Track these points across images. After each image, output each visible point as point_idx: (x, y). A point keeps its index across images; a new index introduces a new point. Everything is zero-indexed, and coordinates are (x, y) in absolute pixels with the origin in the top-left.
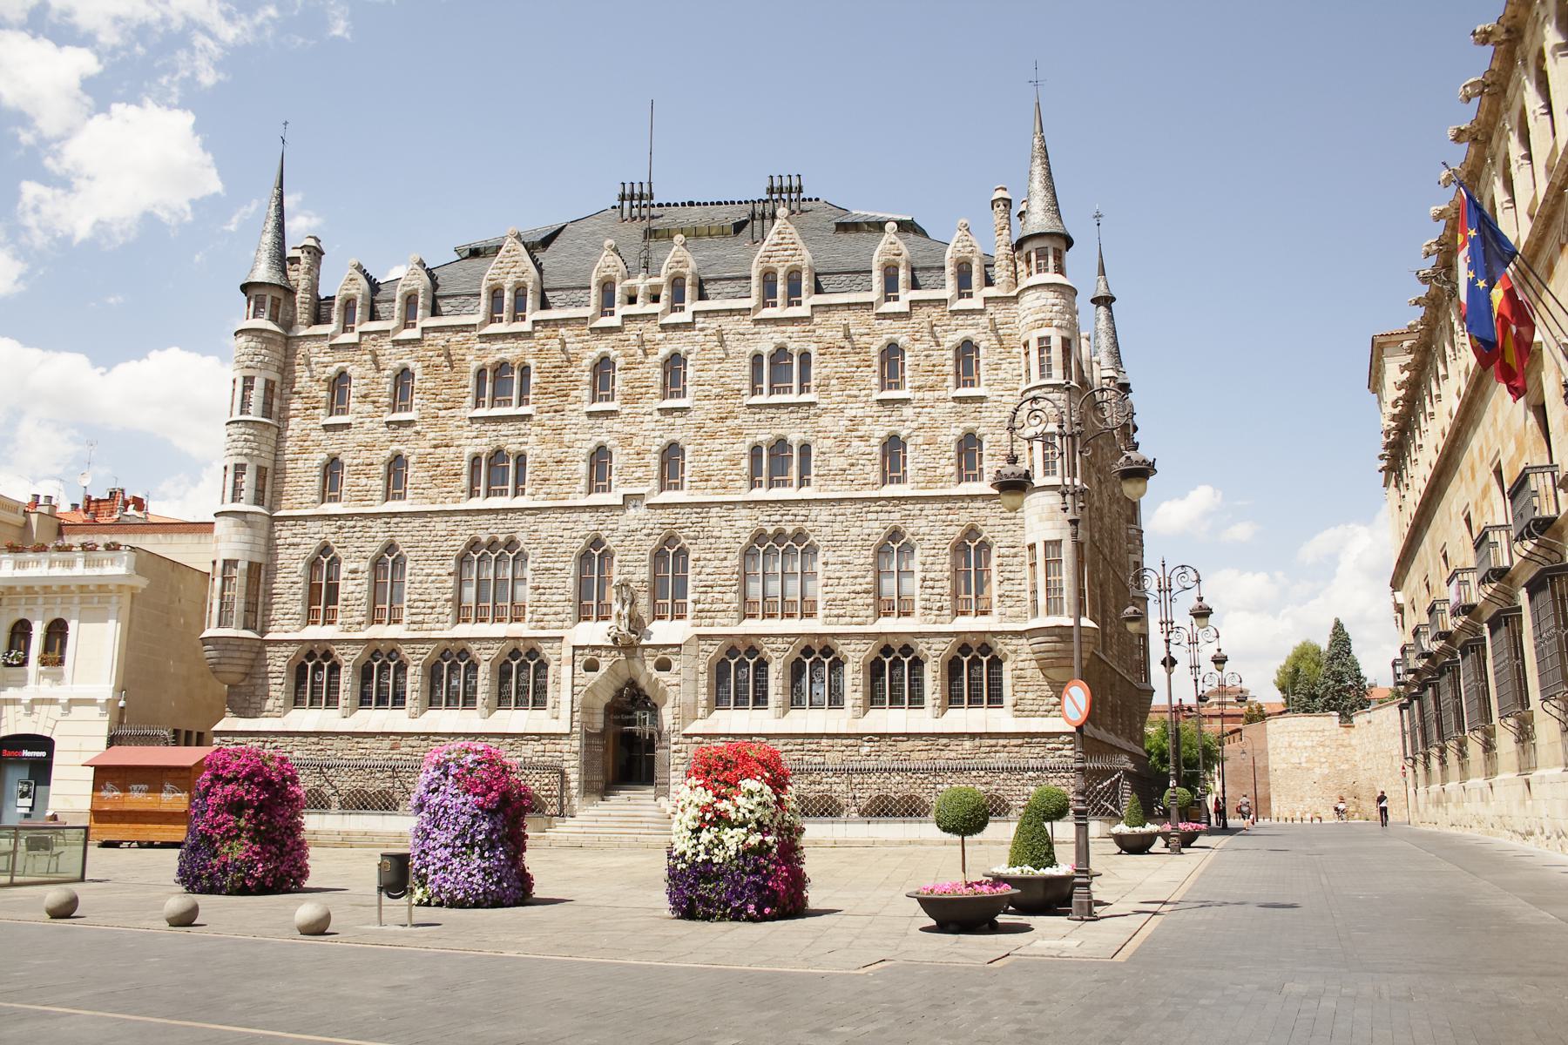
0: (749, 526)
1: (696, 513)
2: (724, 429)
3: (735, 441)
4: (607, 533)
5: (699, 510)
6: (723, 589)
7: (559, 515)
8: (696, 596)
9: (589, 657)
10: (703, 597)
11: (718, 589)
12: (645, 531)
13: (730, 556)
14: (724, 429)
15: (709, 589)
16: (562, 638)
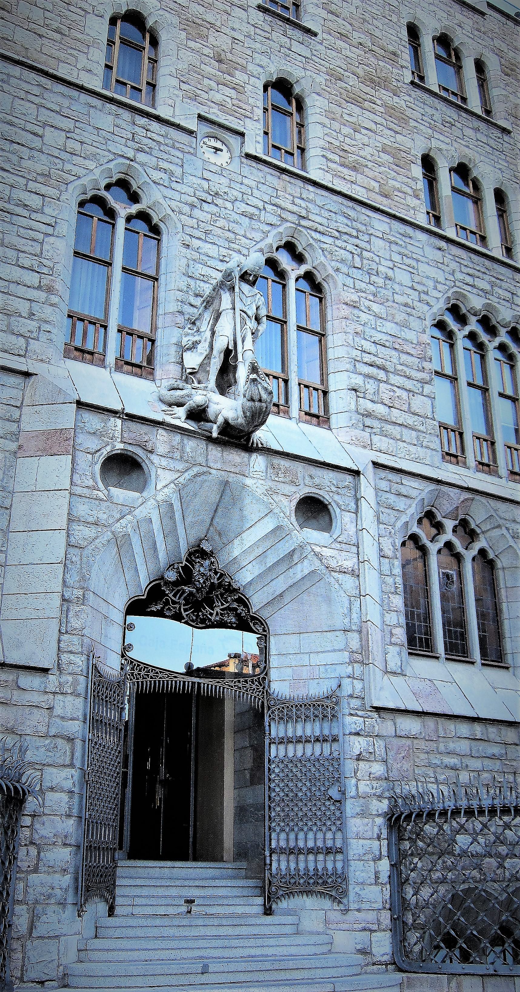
0: (441, 280)
1: (348, 217)
2: (379, 102)
3: (398, 129)
4: (156, 175)
5: (352, 213)
6: (409, 384)
7: (36, 90)
8: (358, 381)
9: (120, 446)
10: (371, 386)
11: (396, 380)
12: (243, 207)
13: (415, 323)
14: (379, 102)
15: (382, 375)
16: (27, 375)
